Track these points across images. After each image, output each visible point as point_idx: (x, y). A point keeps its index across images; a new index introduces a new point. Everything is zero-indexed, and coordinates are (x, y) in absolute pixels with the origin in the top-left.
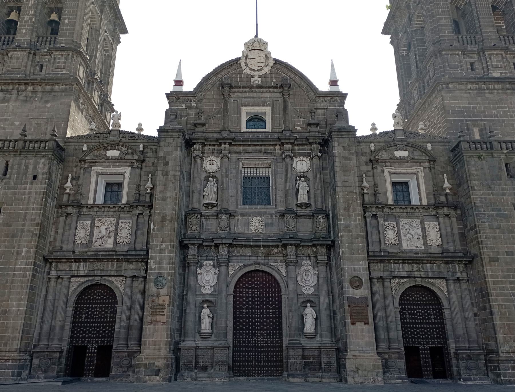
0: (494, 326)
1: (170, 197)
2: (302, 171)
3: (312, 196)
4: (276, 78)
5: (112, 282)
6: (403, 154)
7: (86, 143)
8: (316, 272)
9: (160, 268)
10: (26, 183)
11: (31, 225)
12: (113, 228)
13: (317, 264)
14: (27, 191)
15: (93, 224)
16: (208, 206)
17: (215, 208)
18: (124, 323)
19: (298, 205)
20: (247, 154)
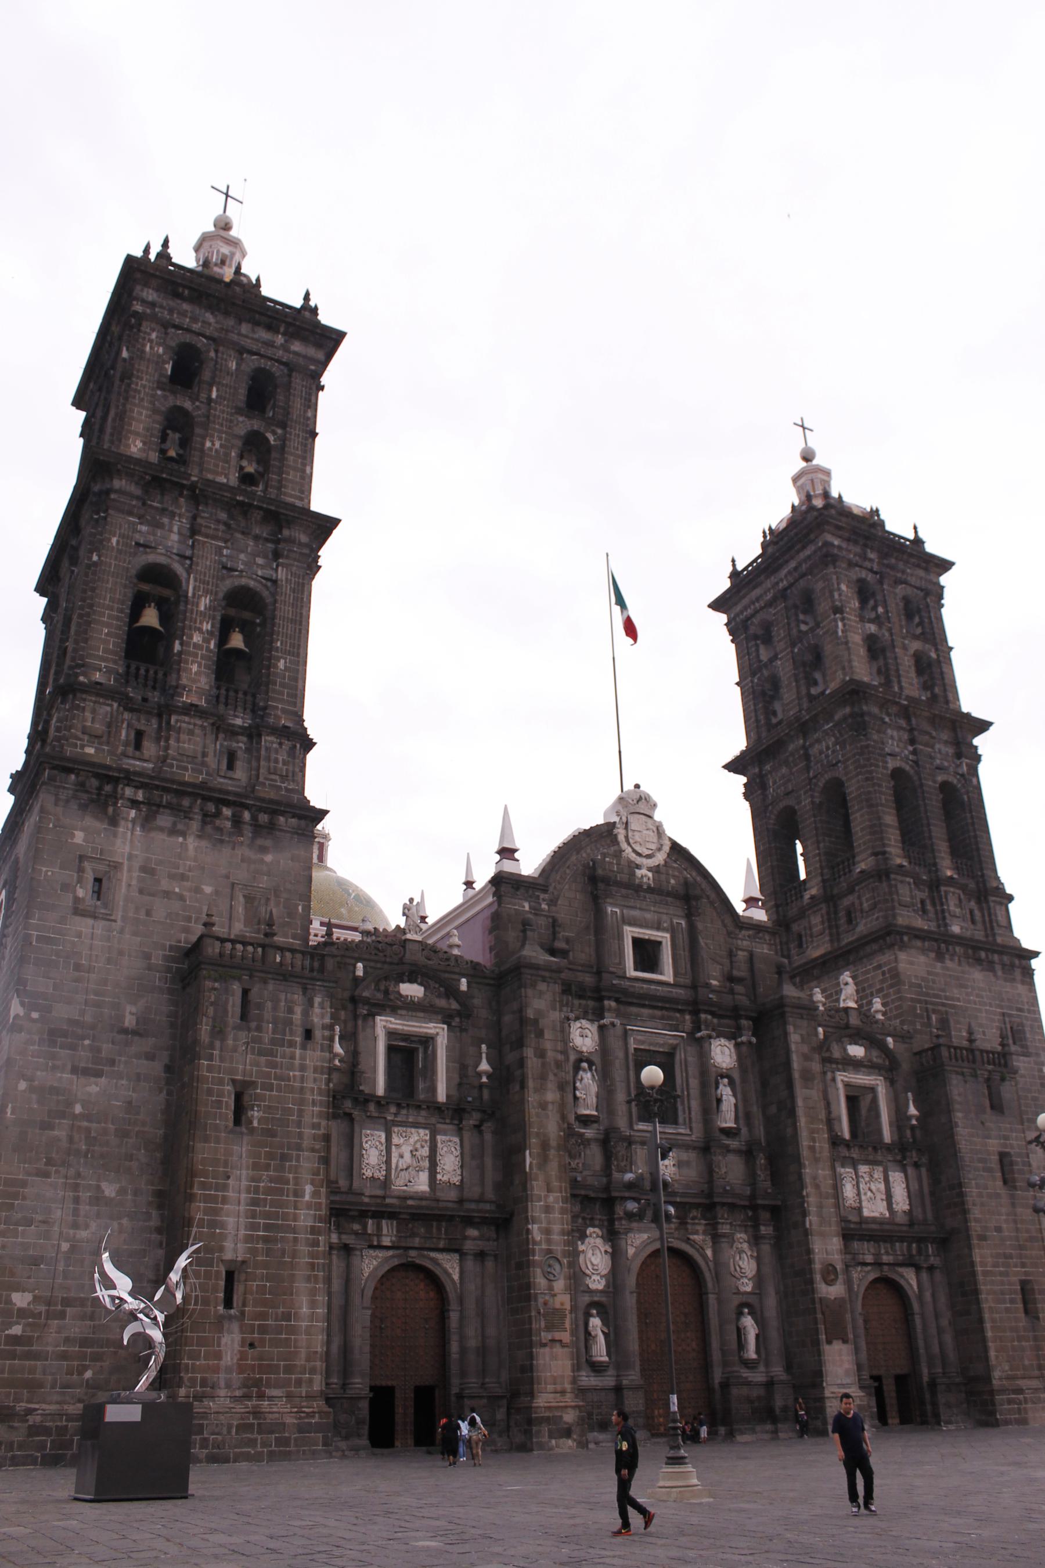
0: (984, 1340)
1: (553, 1103)
2: (724, 1065)
3: (741, 1114)
4: (674, 877)
5: (434, 1261)
6: (856, 1051)
7: (359, 960)
8: (755, 1254)
9: (549, 1241)
10: (292, 1044)
11: (315, 1137)
12: (425, 1151)
13: (756, 1240)
14: (297, 1062)
15: (389, 1139)
16: (586, 1121)
17: (595, 1125)
18: (473, 1343)
19: (723, 1131)
20: (639, 1023)
